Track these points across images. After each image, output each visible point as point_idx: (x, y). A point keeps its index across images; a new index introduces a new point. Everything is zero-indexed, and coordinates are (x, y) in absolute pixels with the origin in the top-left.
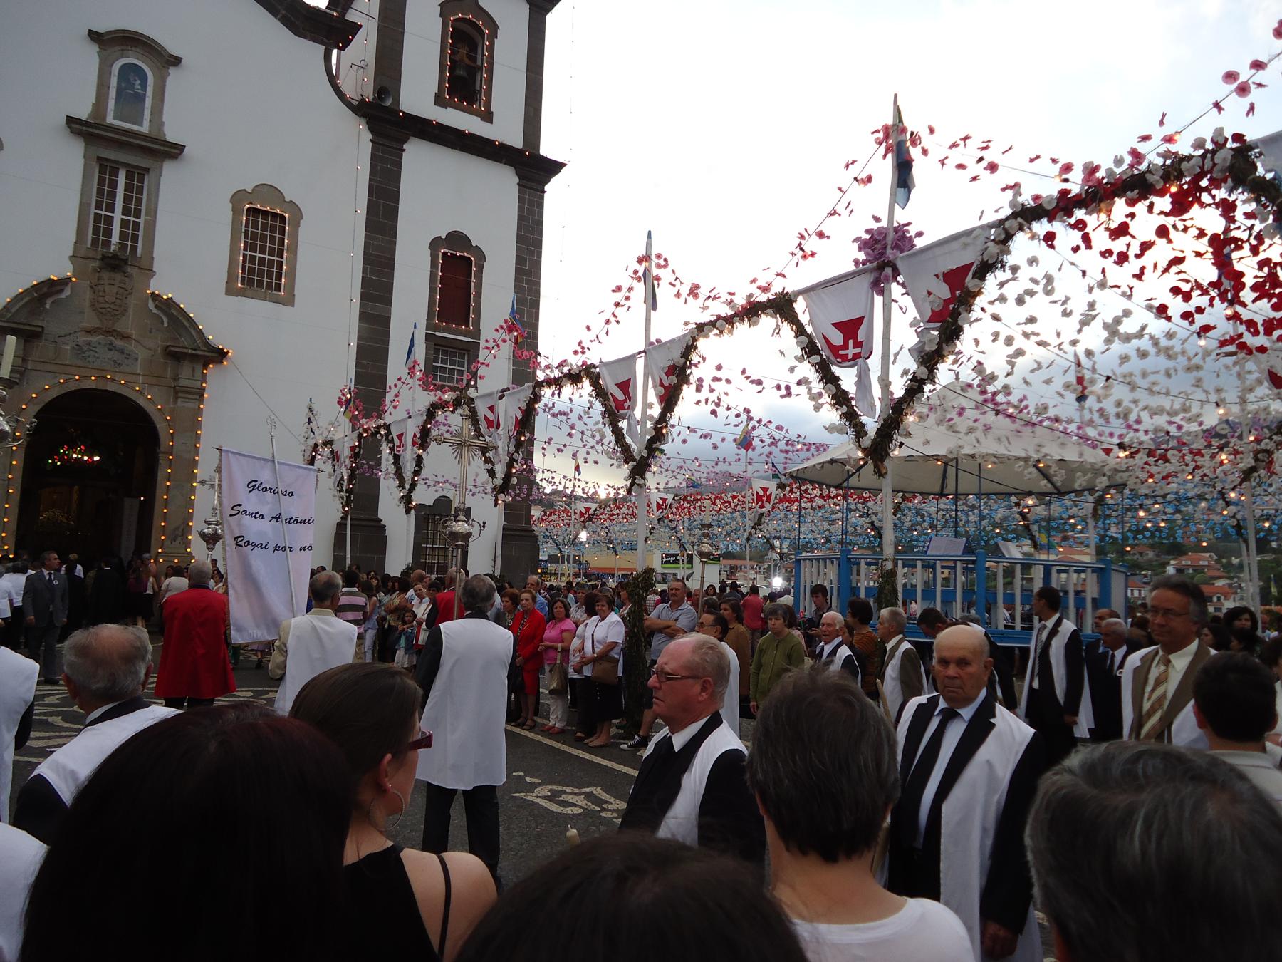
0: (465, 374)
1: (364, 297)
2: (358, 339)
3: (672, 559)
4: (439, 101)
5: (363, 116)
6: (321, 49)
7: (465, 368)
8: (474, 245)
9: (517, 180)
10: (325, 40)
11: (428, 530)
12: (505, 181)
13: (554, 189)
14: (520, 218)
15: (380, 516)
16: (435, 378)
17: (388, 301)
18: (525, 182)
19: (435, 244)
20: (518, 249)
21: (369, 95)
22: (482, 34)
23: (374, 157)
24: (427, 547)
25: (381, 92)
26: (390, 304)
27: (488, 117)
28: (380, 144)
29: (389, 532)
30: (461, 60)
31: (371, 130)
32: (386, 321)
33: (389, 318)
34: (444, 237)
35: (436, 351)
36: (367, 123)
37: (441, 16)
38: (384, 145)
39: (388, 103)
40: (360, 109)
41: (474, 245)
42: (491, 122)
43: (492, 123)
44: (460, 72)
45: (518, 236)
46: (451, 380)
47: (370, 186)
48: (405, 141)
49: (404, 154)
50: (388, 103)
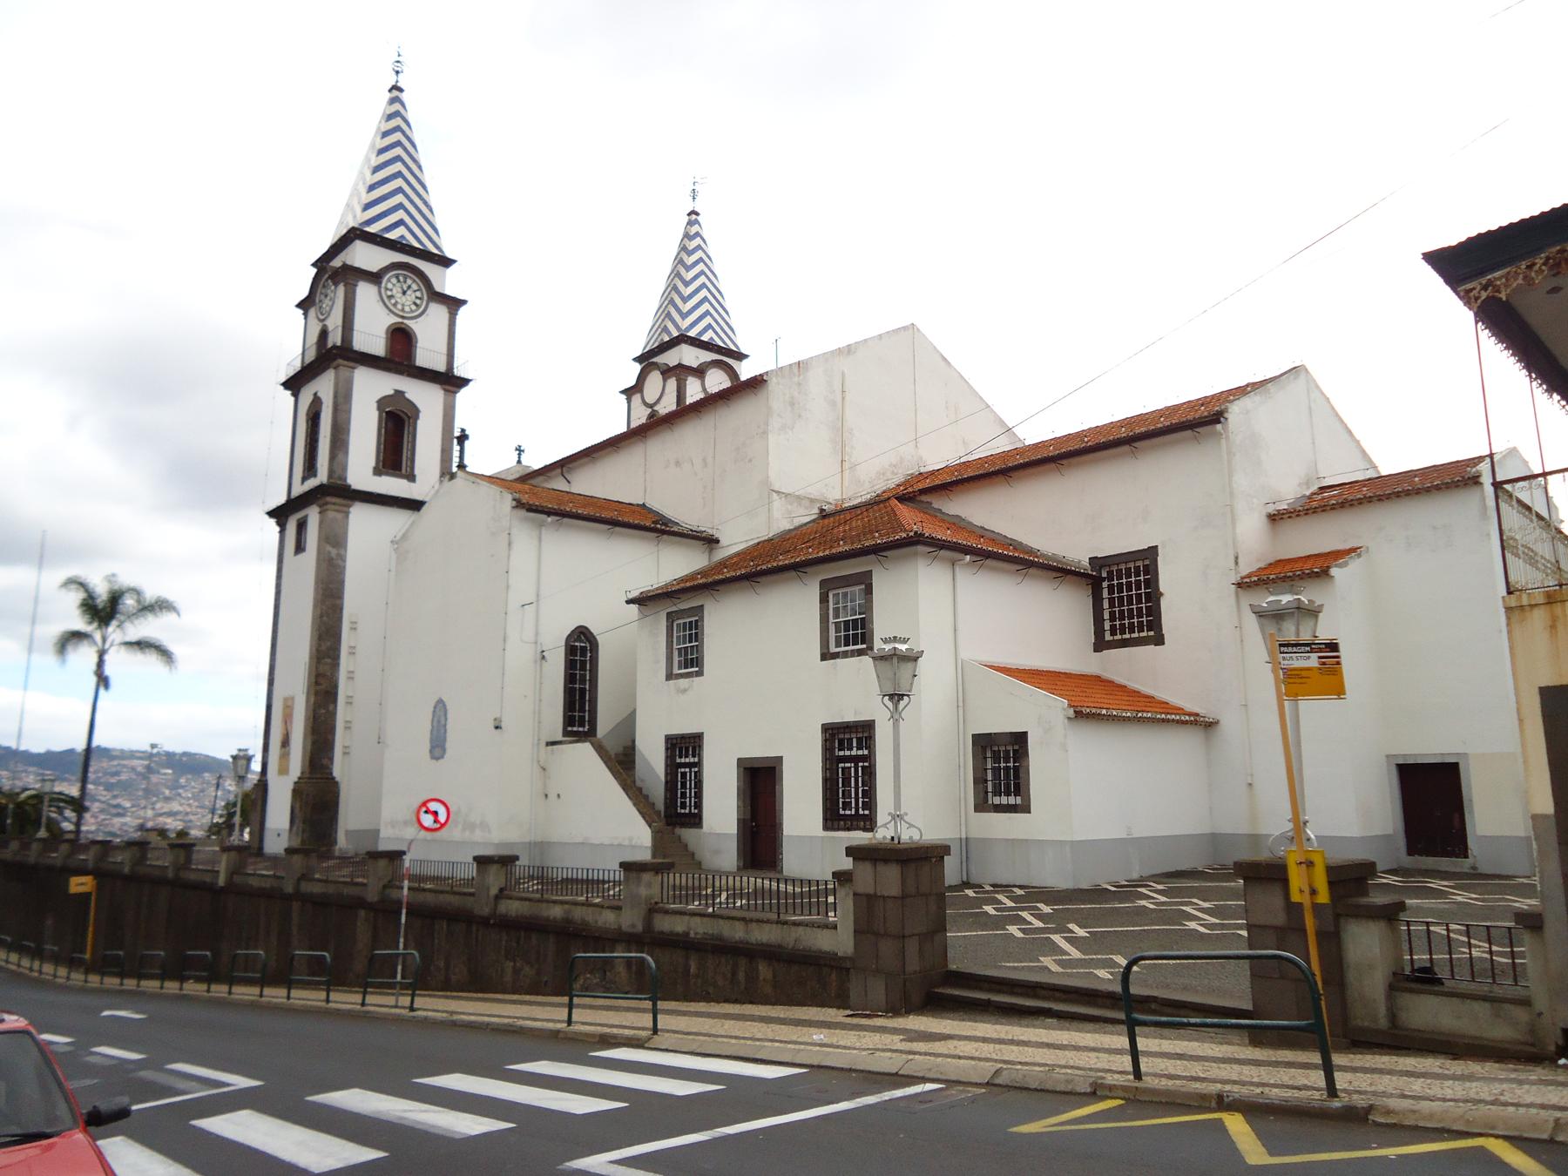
4: (377, 471)
27: (411, 477)
49: (351, 516)
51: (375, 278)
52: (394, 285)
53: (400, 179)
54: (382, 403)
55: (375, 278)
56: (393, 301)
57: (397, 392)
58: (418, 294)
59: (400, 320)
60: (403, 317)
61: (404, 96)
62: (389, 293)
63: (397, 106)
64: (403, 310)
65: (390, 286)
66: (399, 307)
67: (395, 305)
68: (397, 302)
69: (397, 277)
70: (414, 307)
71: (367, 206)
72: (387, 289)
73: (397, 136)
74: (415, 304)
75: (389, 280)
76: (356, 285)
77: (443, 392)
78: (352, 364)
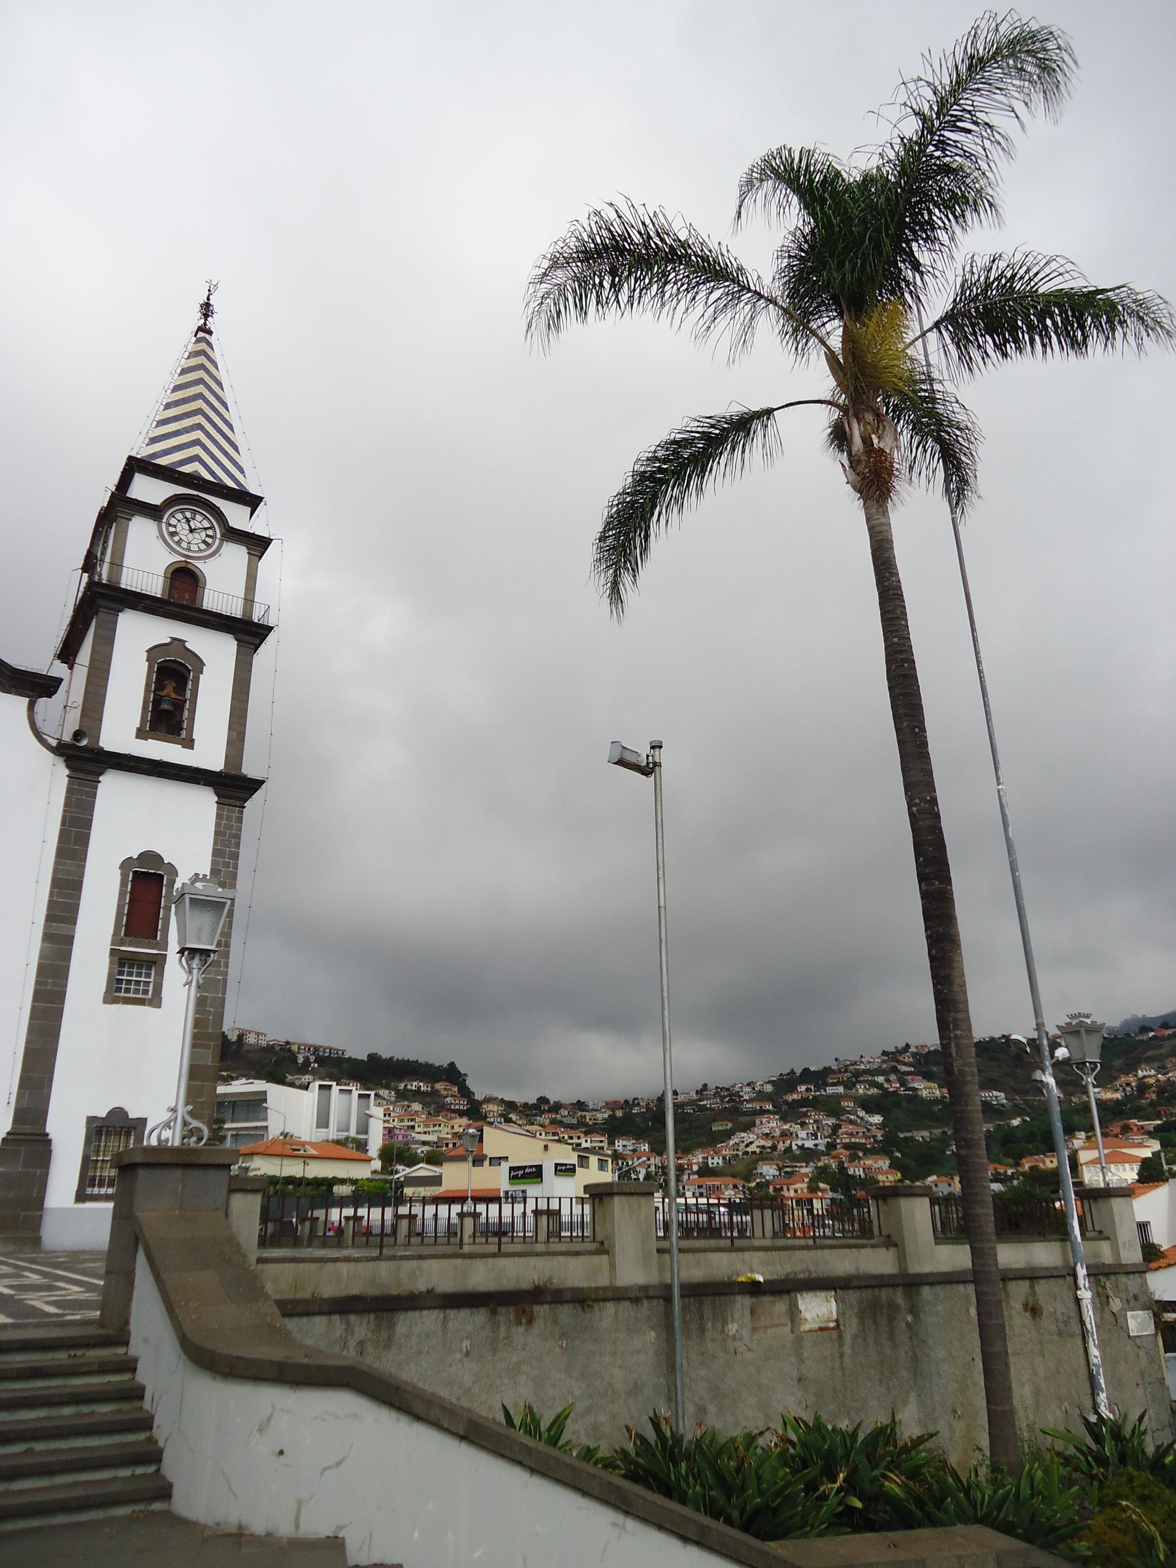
0: (151, 985)
1: (50, 918)
2: (41, 958)
3: (521, 1172)
4: (141, 734)
5: (61, 755)
6: (25, 701)
7: (152, 980)
8: (166, 862)
9: (216, 799)
10: (30, 693)
11: (100, 1141)
12: (205, 801)
13: (254, 804)
14: (217, 833)
15: (47, 1130)
16: (119, 990)
17: (73, 921)
18: (223, 800)
19: (126, 864)
20: (213, 863)
21: (67, 737)
22: (189, 671)
23: (69, 790)
24: (97, 1161)
25: (78, 735)
26: (75, 924)
27: (189, 743)
28: (78, 778)
29: (56, 1147)
30: (168, 696)
31: (68, 767)
32: (69, 940)
33: (73, 937)
34: (135, 857)
35: (122, 965)
36: (65, 761)
37: (147, 661)
38: (78, 778)
39: (84, 743)
40: (61, 750)
41: (166, 862)
42: (193, 749)
43: (193, 749)
44: (165, 706)
45: (213, 848)
46: (137, 991)
47: (64, 817)
48: (101, 774)
49: (99, 785)
50: (84, 743)
51: (153, 512)
52: (179, 521)
53: (200, 416)
54: (152, 652)
55: (153, 512)
56: (176, 539)
57: (174, 639)
58: (210, 532)
59: (184, 559)
60: (187, 557)
61: (213, 339)
62: (172, 529)
63: (203, 346)
64: (189, 549)
65: (173, 521)
66: (184, 545)
67: (179, 543)
68: (181, 539)
69: (182, 511)
70: (203, 546)
71: (154, 440)
72: (170, 525)
73: (201, 374)
74: (204, 542)
75: (172, 515)
76: (131, 520)
77: (236, 643)
78: (114, 605)
